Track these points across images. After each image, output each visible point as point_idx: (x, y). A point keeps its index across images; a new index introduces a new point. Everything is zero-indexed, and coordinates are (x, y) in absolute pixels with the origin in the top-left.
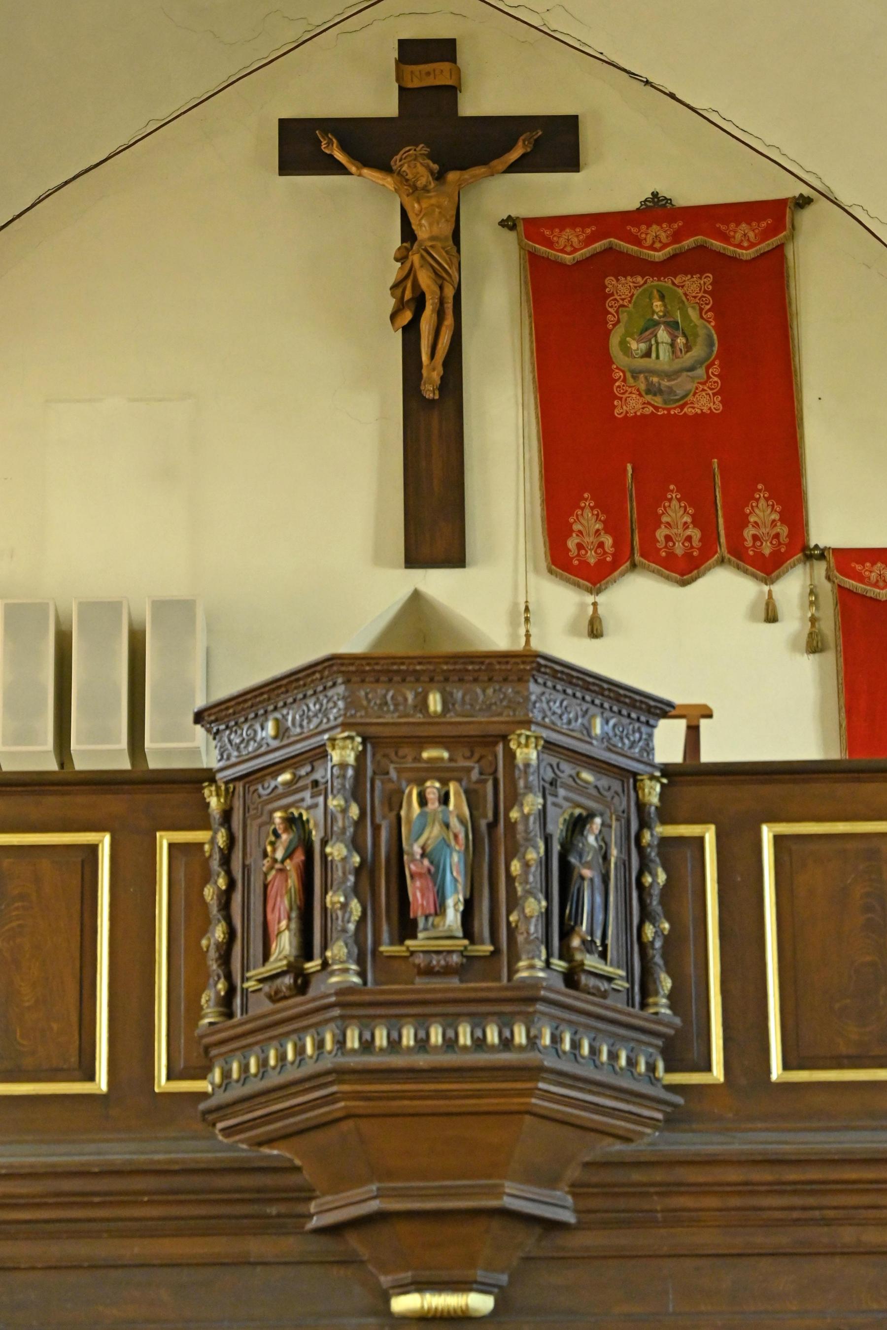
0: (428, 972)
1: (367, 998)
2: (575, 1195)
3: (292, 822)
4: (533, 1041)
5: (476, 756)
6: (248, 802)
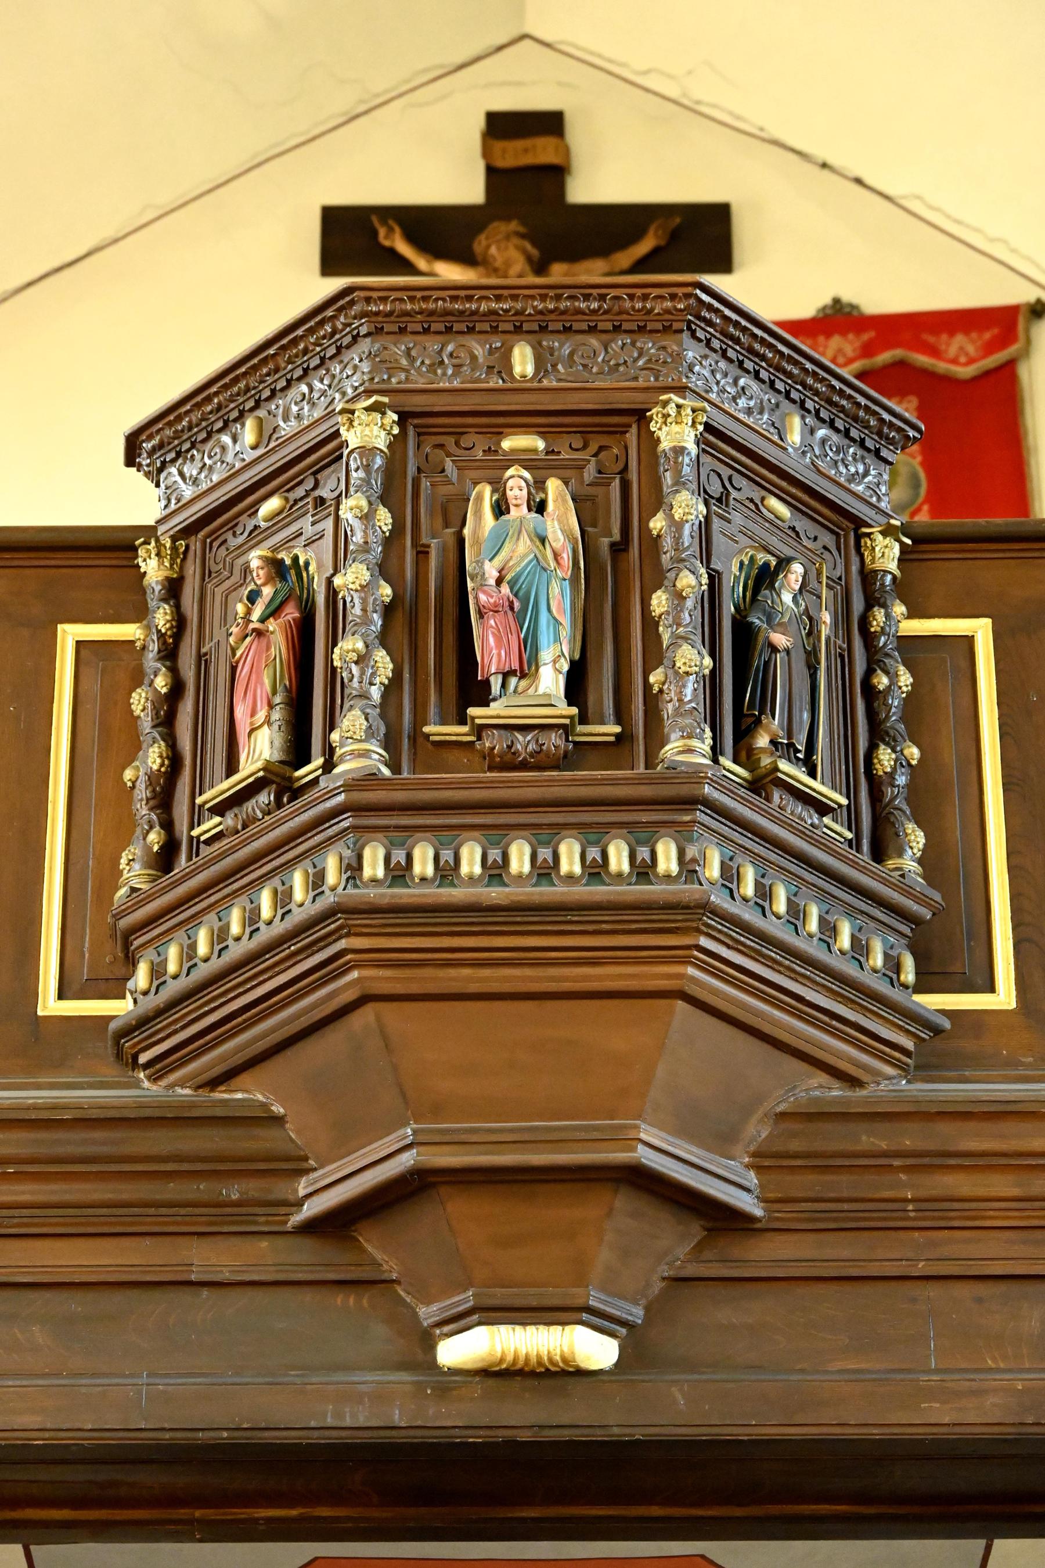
0: (509, 763)
1: (400, 796)
2: (759, 1169)
3: (277, 569)
4: (689, 869)
5: (593, 447)
6: (211, 564)
